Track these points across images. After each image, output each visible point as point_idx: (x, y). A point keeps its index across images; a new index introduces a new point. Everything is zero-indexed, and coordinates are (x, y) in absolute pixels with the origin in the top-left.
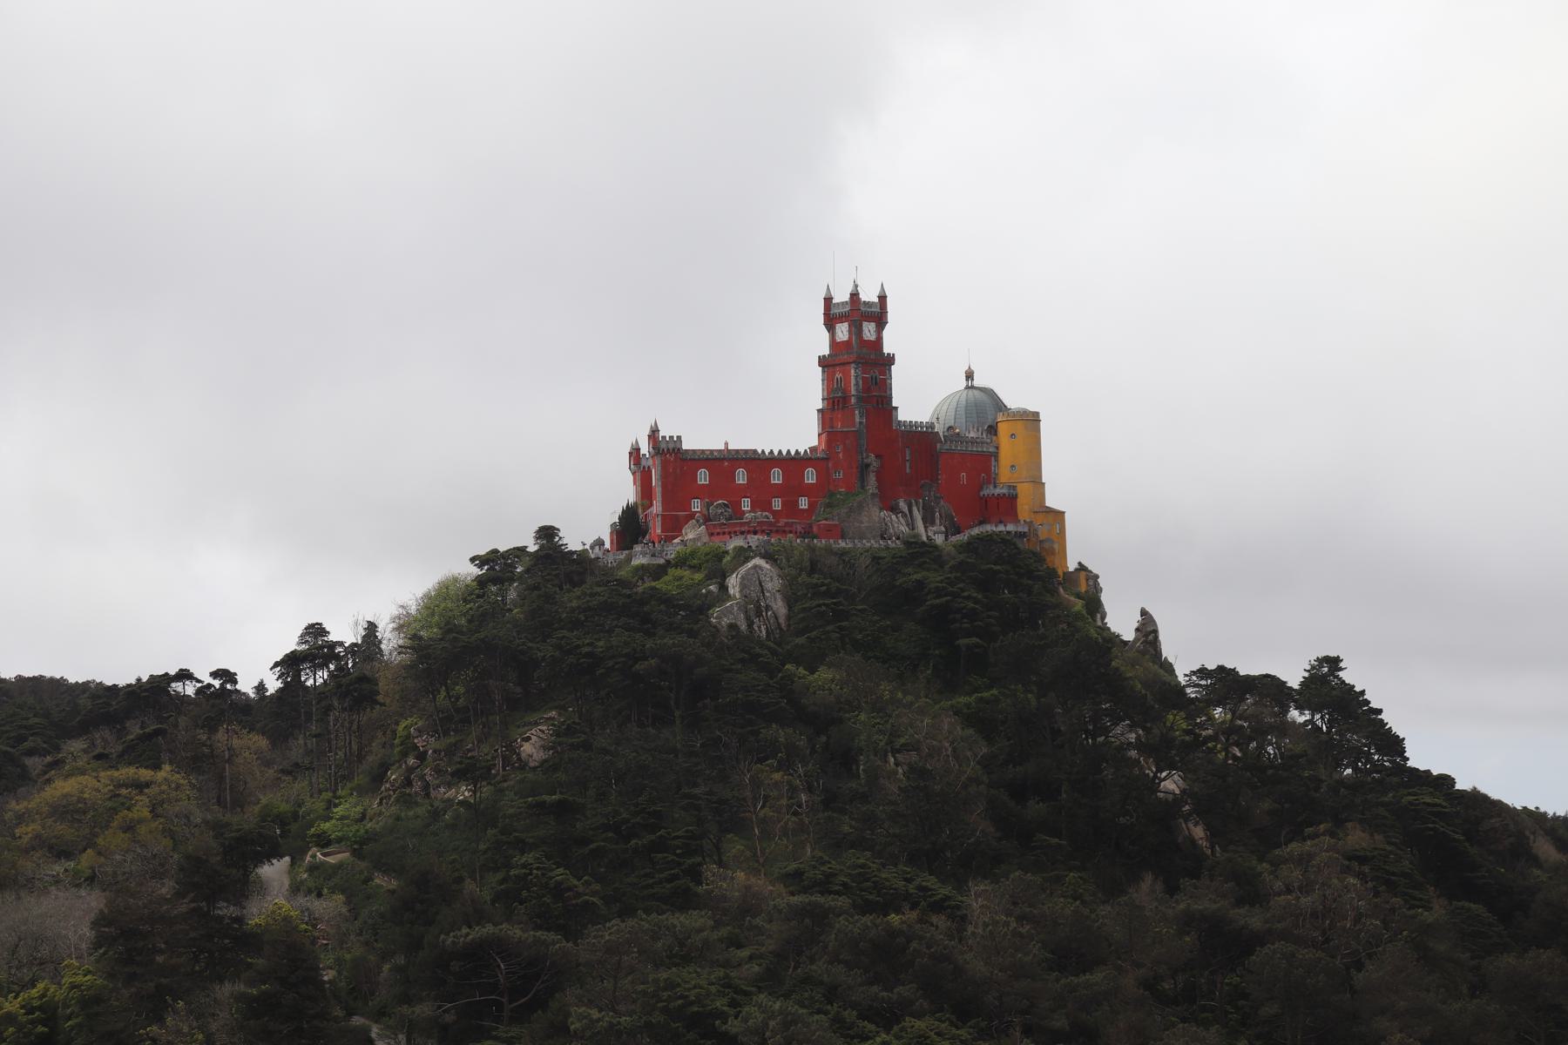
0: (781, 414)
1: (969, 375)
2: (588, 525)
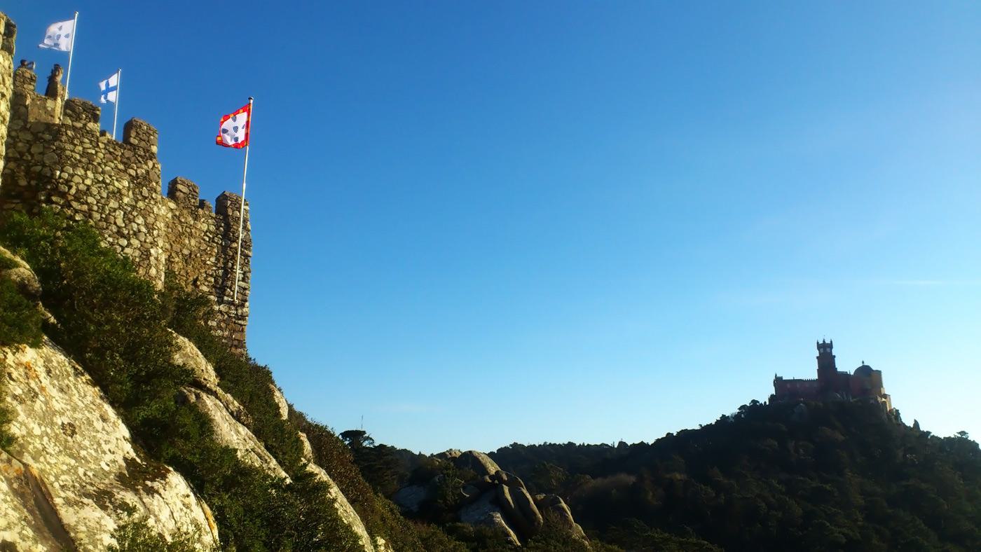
0: (809, 372)
1: (863, 362)
2: (763, 399)
